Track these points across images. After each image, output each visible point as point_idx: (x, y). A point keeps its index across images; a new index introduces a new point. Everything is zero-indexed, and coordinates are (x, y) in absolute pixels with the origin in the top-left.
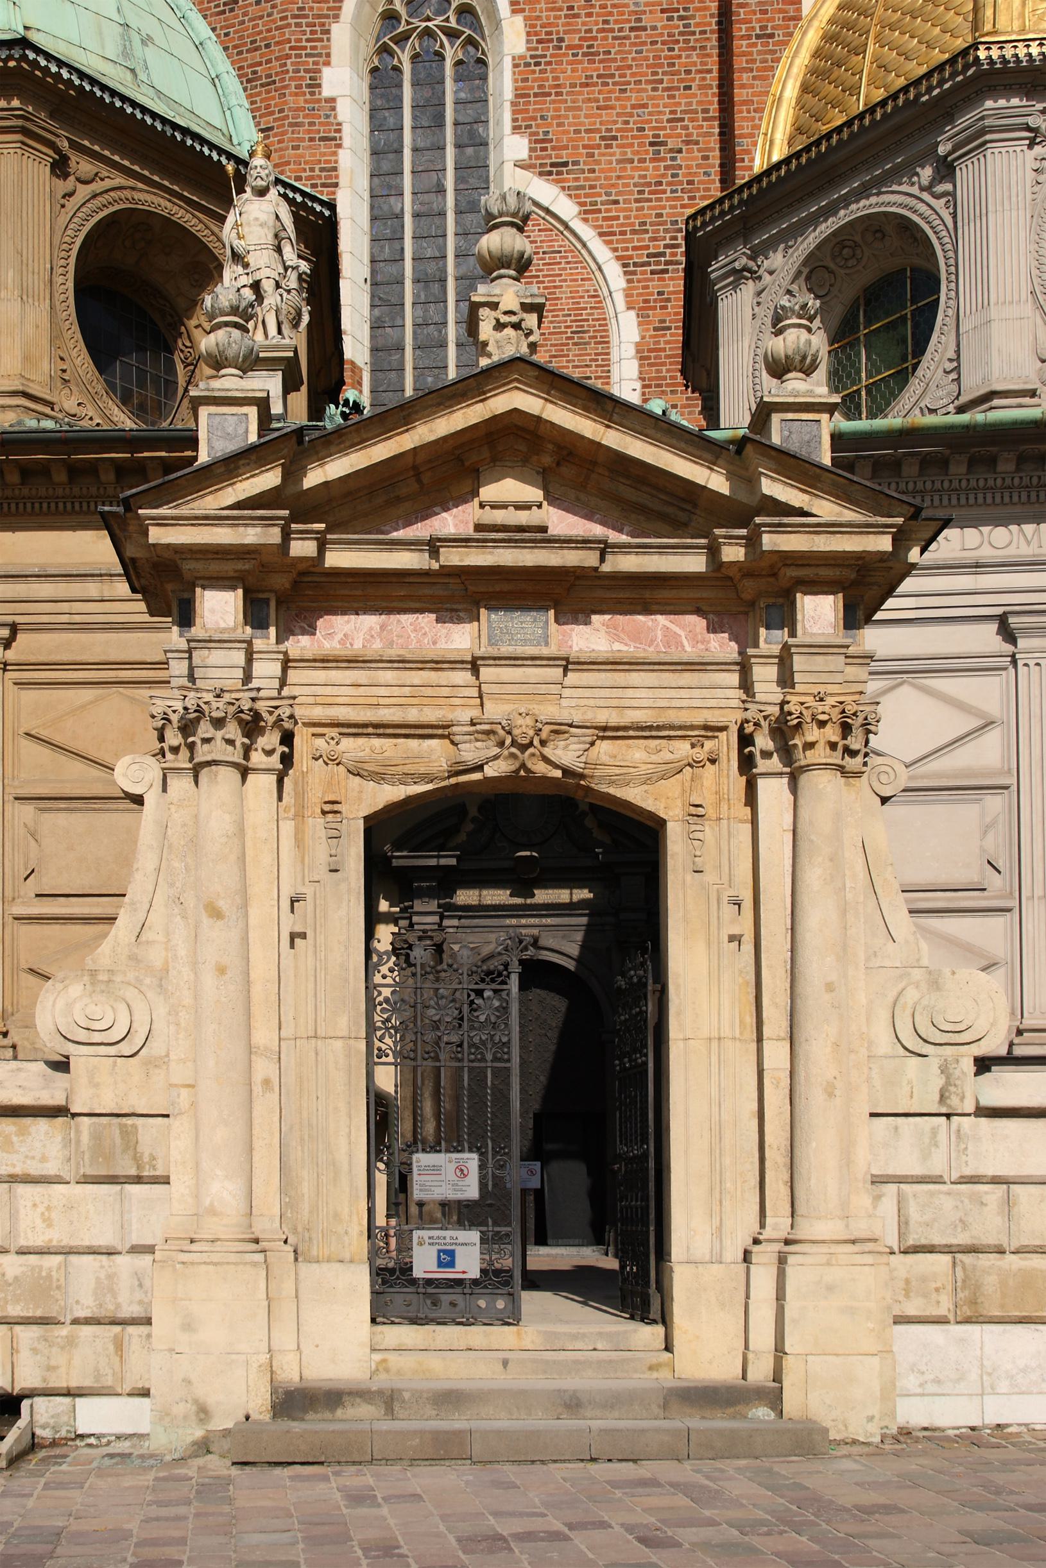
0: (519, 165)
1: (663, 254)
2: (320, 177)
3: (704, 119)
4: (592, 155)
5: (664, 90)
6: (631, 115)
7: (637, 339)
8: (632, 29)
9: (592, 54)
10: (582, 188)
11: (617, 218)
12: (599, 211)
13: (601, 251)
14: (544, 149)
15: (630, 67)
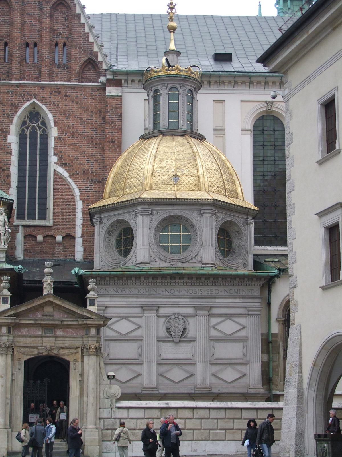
0: (55, 163)
1: (89, 187)
2: (6, 162)
3: (99, 155)
4: (73, 162)
5: (90, 148)
6: (82, 153)
7: (82, 207)
8: (83, 132)
9: (74, 138)
10: (70, 170)
11: (78, 178)
12: (74, 176)
13: (74, 186)
14: (61, 160)
15: (82, 142)
